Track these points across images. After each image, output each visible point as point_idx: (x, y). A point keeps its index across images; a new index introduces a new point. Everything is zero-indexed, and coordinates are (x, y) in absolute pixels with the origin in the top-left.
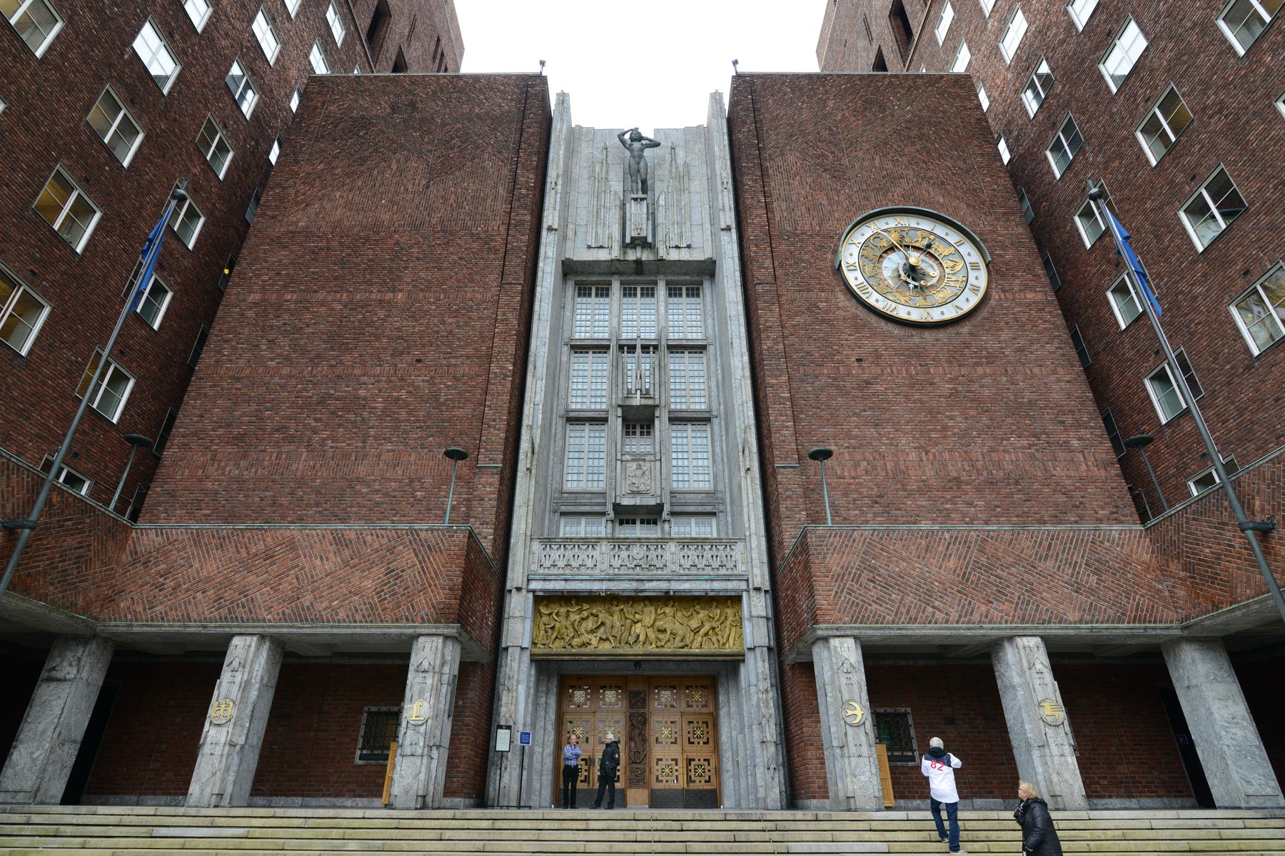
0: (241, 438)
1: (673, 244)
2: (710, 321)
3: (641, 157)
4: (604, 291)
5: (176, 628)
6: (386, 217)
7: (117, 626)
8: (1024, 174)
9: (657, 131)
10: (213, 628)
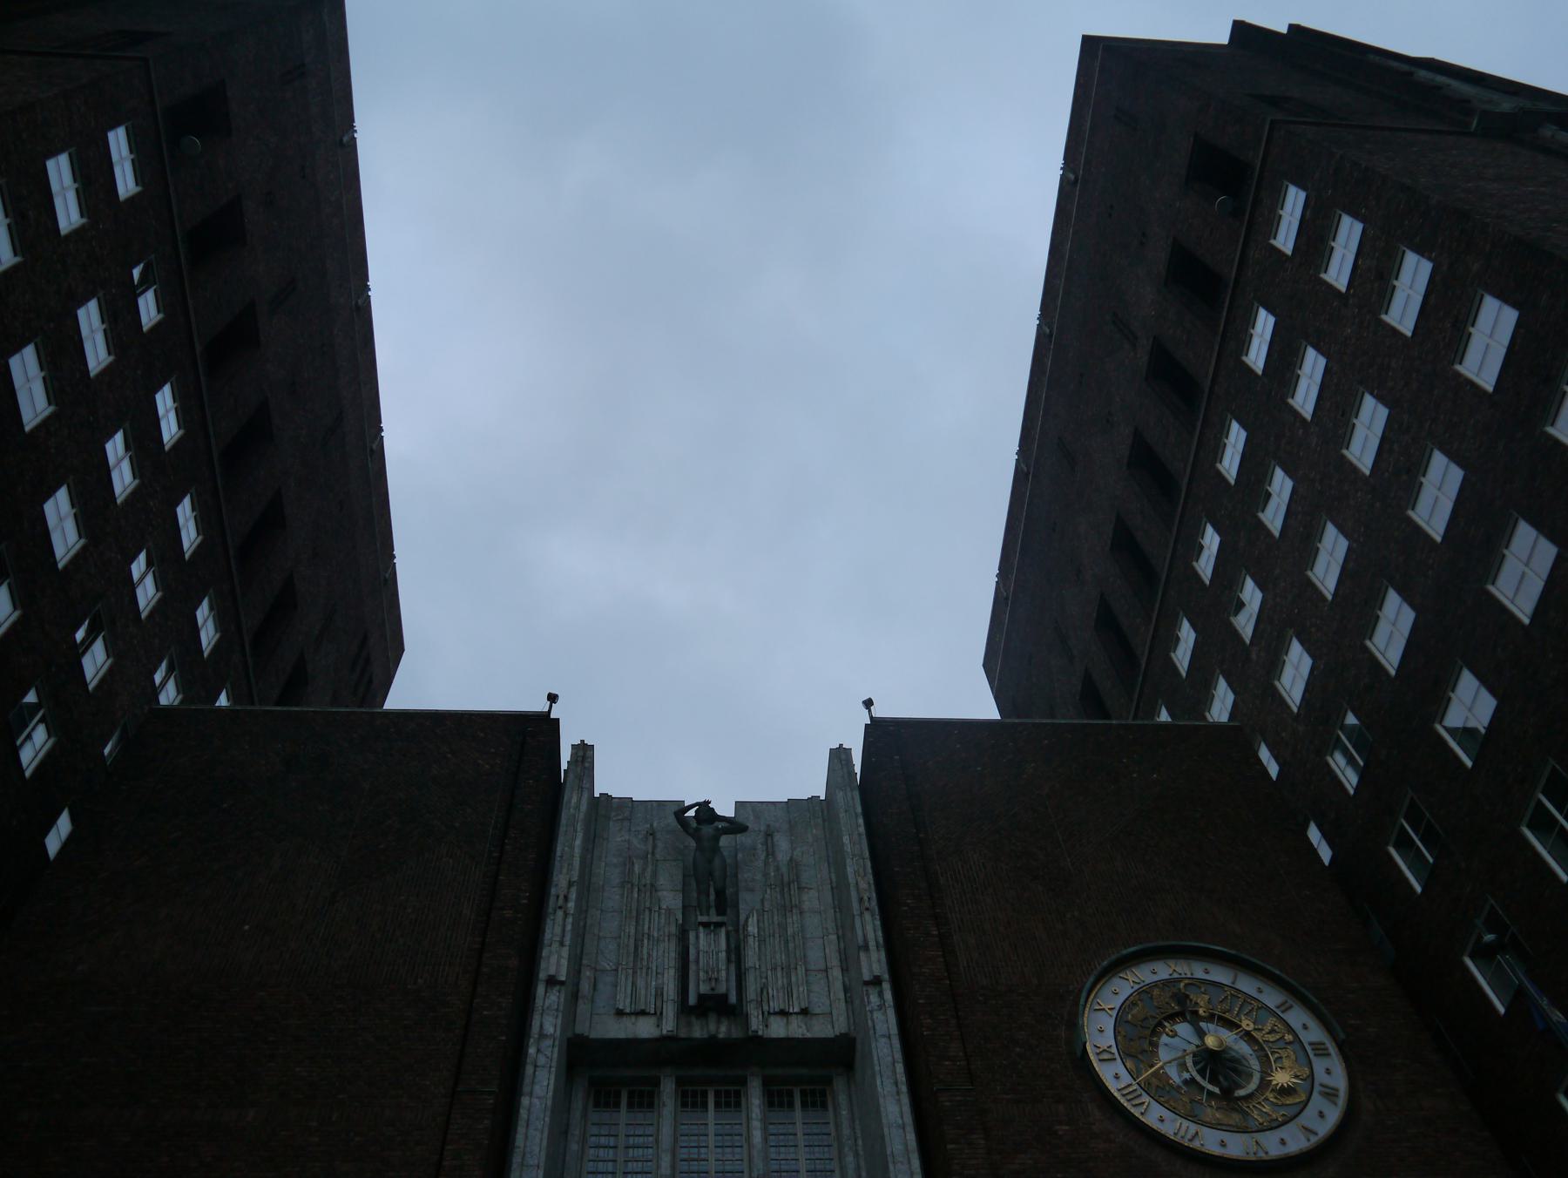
1: (775, 1005)
2: (850, 1159)
3: (716, 849)
9: (740, 805)
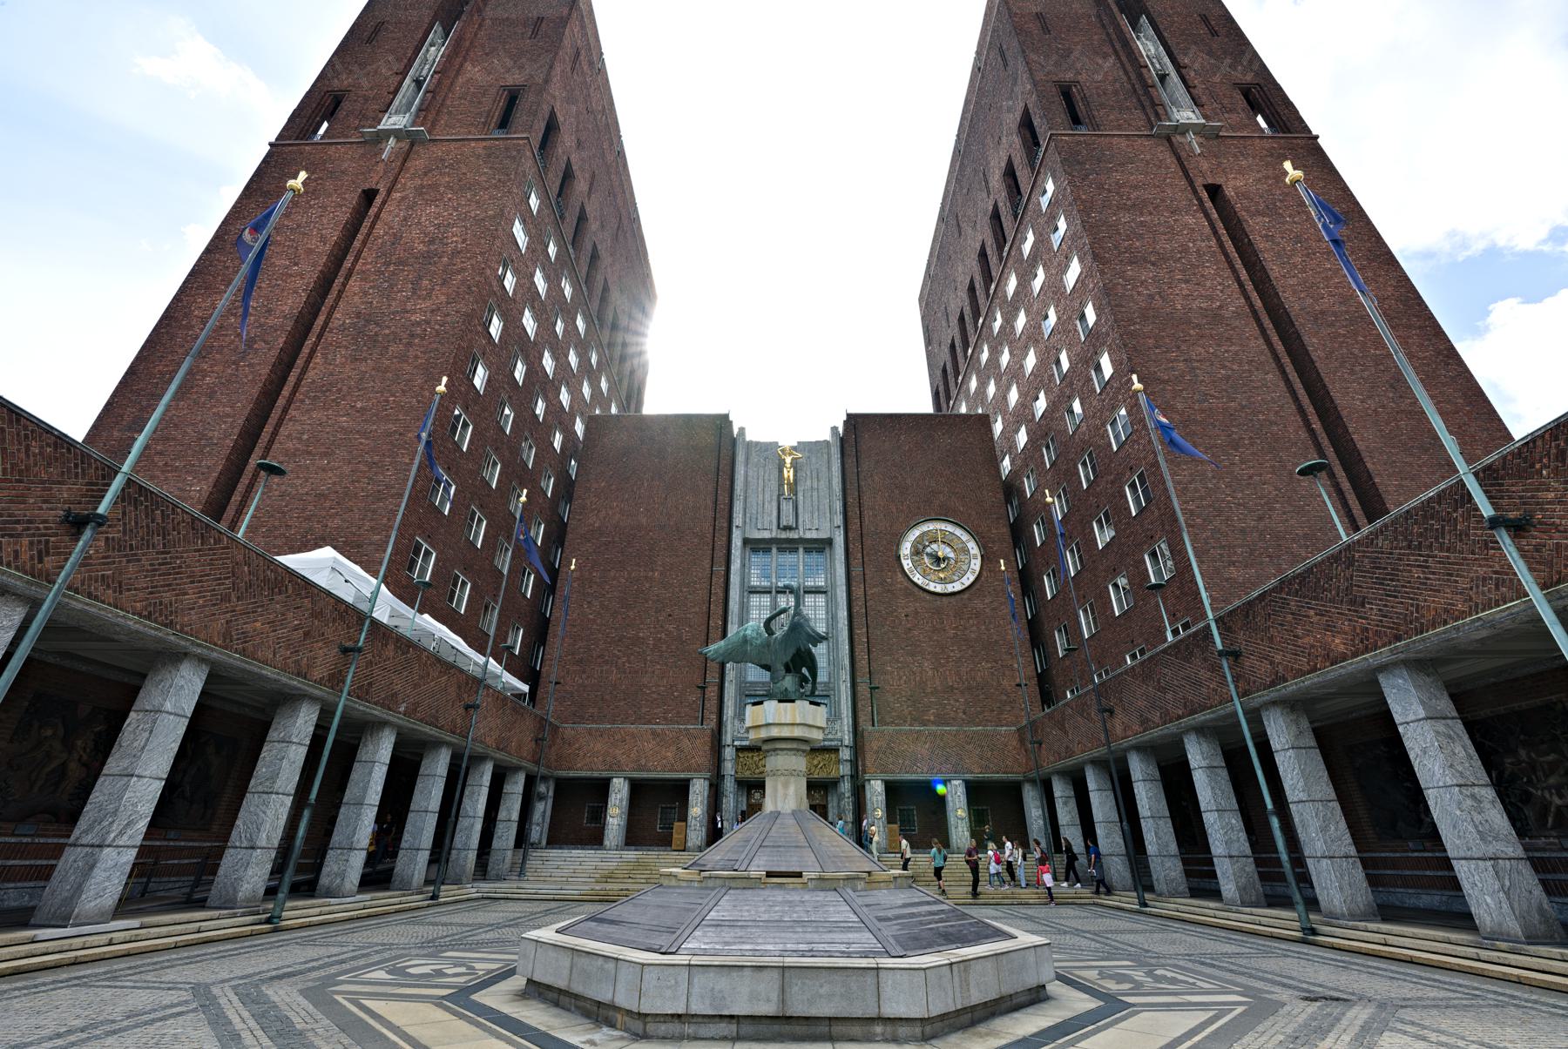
0: (581, 661)
4: (768, 550)
5: (588, 774)
6: (644, 521)
7: (563, 774)
8: (1010, 489)
10: (605, 774)
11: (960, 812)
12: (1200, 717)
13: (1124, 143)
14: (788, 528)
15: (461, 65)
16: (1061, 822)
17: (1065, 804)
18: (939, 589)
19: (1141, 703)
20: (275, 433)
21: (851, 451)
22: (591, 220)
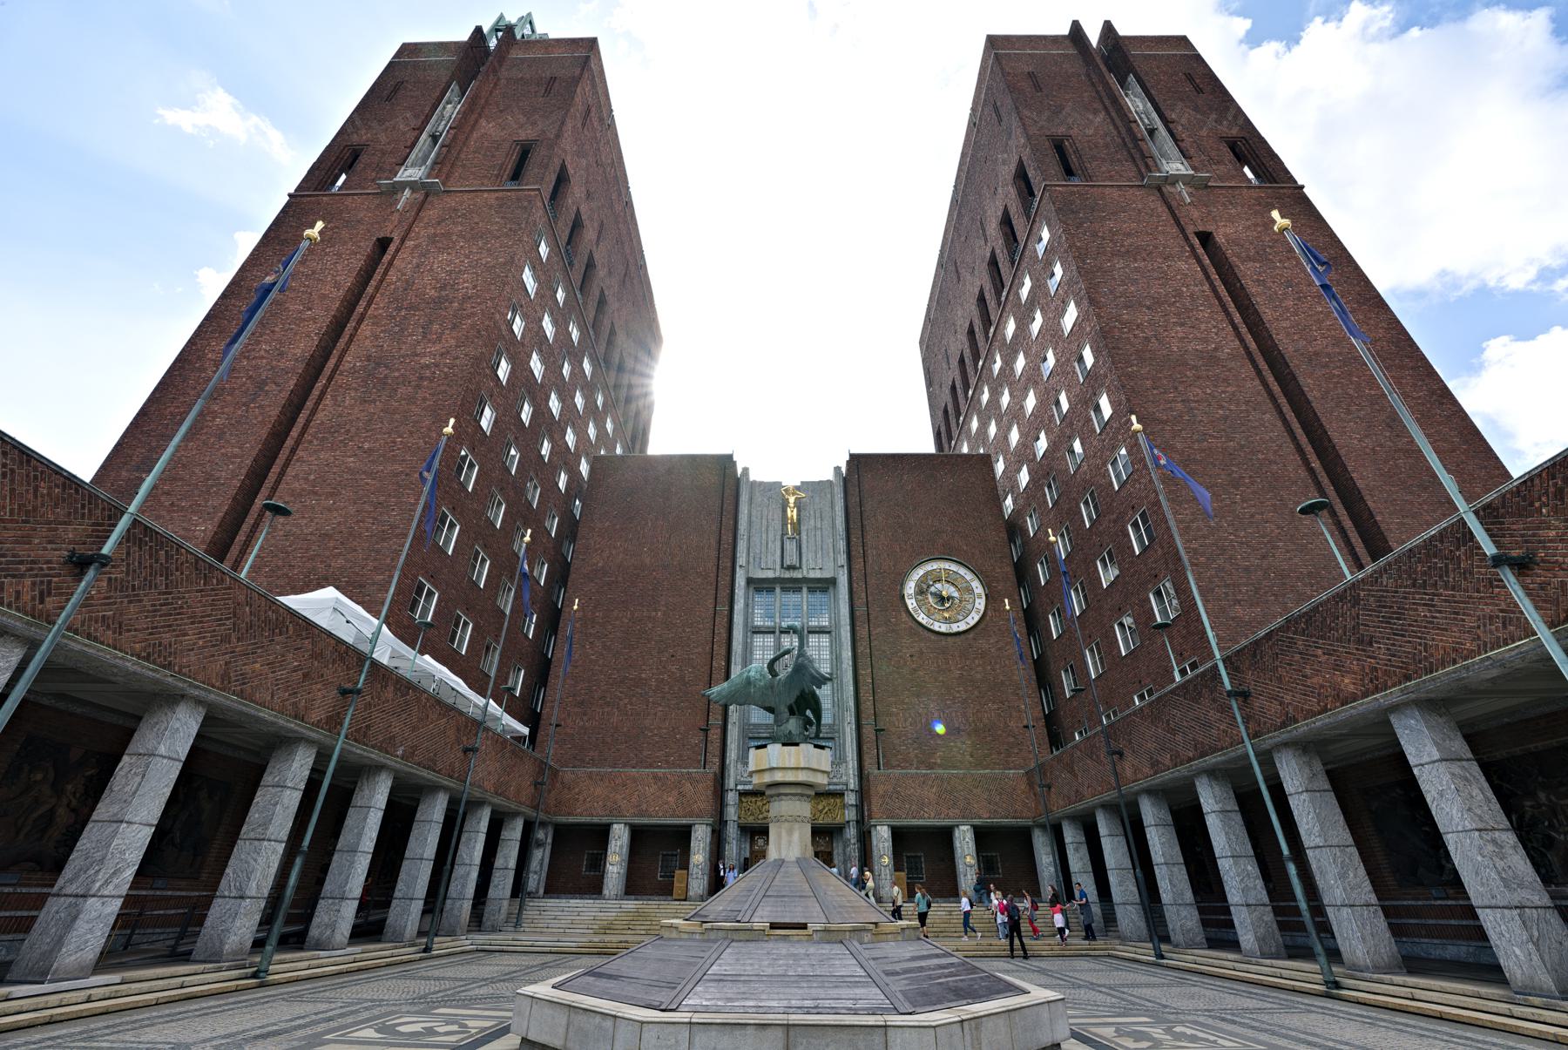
0: (582, 703)
4: (772, 590)
6: (647, 561)
8: (1013, 528)
10: (605, 820)
11: (968, 859)
12: (1211, 760)
13: (1116, 193)
14: (791, 568)
15: (477, 121)
16: (1072, 869)
17: (1076, 850)
18: (944, 628)
19: (1151, 746)
20: (282, 473)
21: (854, 491)
22: (599, 267)
